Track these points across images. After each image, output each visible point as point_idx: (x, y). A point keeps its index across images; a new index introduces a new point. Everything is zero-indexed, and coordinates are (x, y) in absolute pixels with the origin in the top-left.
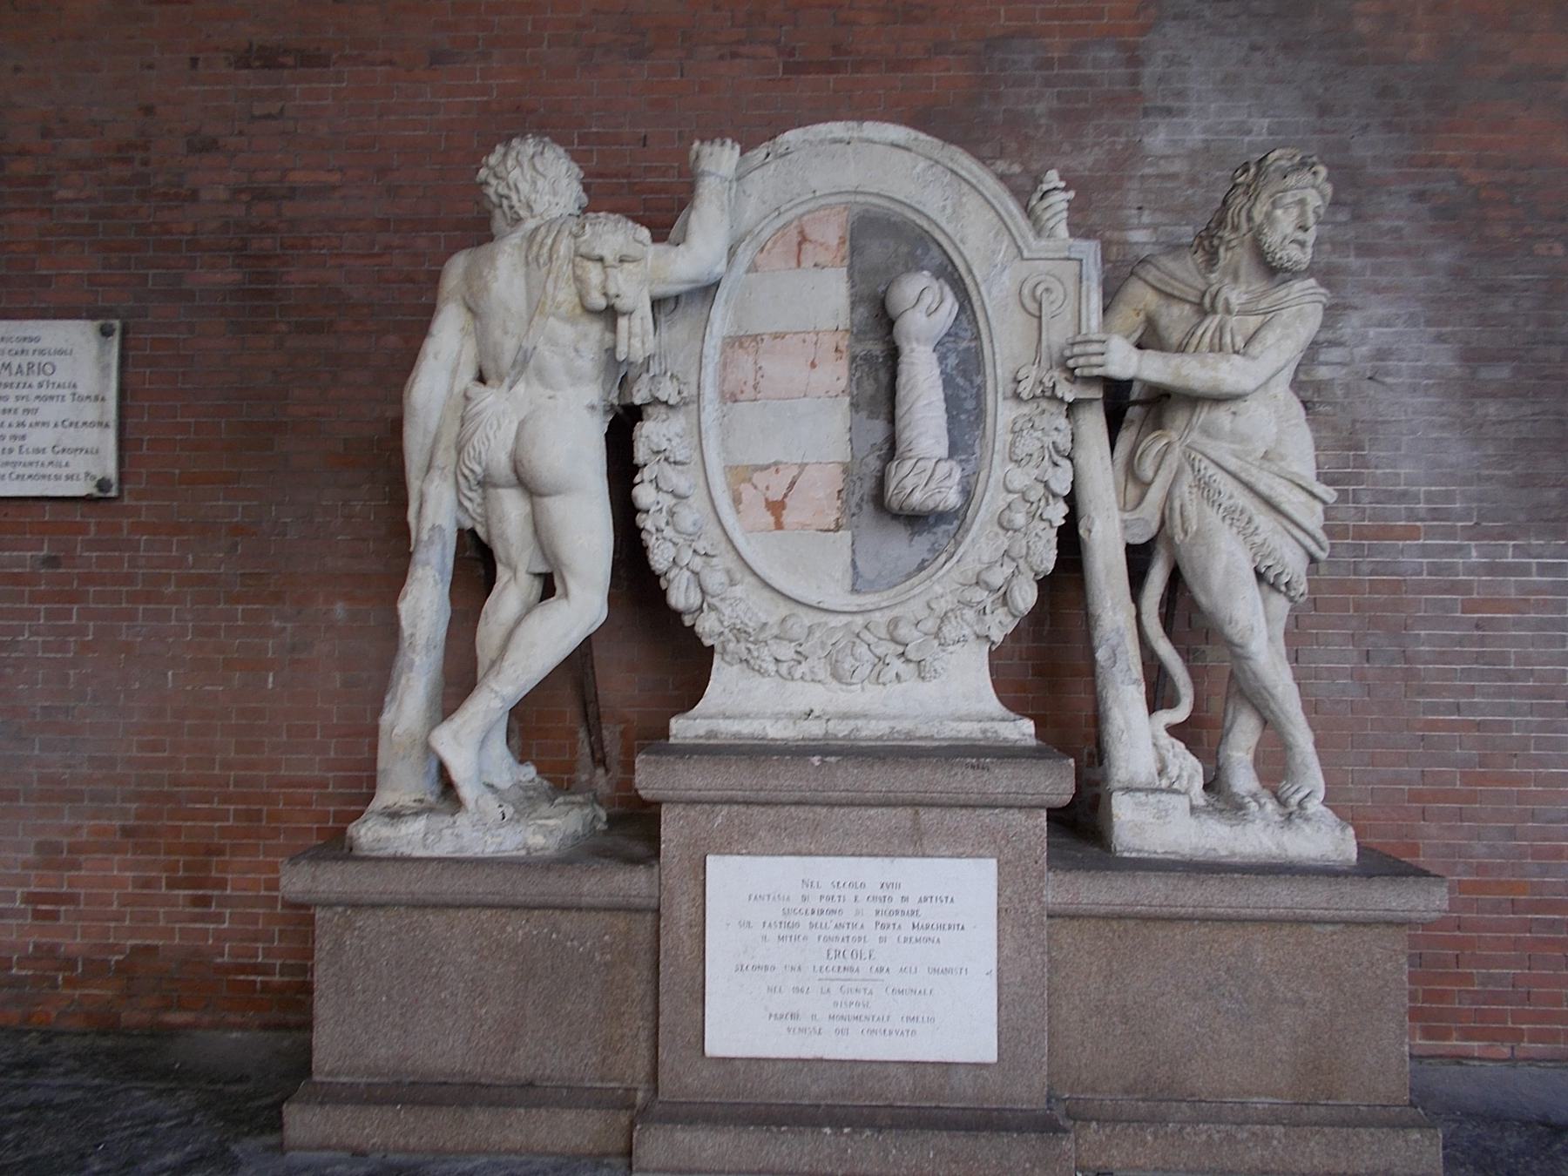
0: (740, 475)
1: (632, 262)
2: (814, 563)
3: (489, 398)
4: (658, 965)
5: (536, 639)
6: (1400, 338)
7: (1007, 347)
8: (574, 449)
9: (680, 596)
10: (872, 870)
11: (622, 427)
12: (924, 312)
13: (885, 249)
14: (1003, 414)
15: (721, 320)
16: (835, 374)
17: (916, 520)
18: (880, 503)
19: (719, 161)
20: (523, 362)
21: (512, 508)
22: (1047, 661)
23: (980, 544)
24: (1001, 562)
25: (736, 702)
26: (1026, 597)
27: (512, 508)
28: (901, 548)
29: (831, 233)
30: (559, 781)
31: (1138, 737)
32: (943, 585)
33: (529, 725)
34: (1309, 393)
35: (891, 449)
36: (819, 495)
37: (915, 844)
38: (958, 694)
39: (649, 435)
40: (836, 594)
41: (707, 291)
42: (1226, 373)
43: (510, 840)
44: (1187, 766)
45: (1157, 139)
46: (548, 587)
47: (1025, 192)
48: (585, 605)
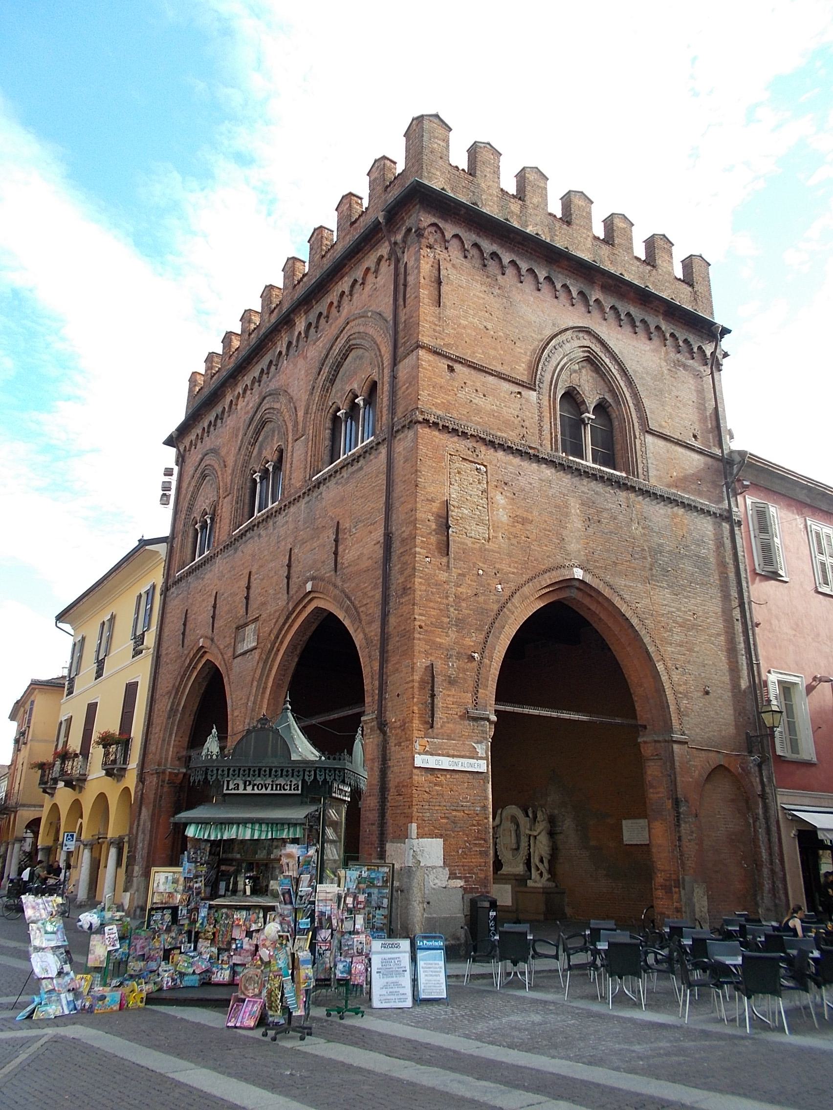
44: (538, 877)
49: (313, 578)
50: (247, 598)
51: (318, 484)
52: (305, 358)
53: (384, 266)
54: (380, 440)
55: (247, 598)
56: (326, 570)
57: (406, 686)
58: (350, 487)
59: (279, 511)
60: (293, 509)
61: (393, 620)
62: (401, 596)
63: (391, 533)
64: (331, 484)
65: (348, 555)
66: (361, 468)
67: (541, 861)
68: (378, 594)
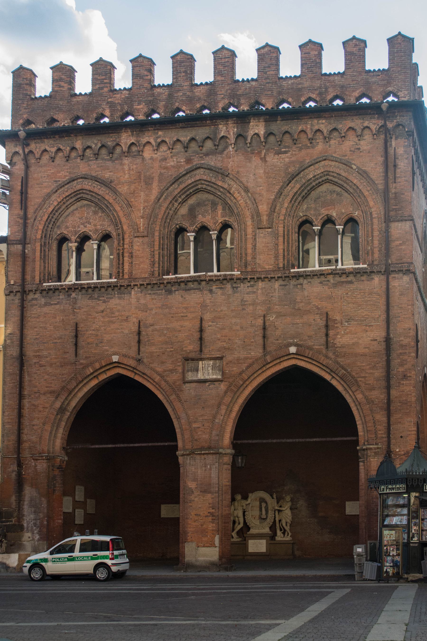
0: (252, 516)
1: (244, 503)
2: (257, 522)
3: (235, 511)
4: (246, 546)
5: (238, 527)
6: (302, 504)
7: (270, 507)
8: (241, 514)
9: (248, 524)
10: (258, 541)
11: (244, 512)
12: (264, 505)
13: (262, 500)
14: (270, 511)
15: (251, 505)
16: (258, 509)
17: (264, 519)
18: (260, 518)
19: (250, 495)
20: (237, 509)
21: (237, 518)
22: (273, 528)
23: (268, 520)
24: (270, 521)
25: (253, 531)
26: (271, 524)
27: (237, 518)
28: (263, 521)
29: (258, 499)
30: (240, 537)
31: (279, 533)
32: (266, 523)
33: (238, 533)
34: (291, 509)
35: (262, 514)
36: (257, 517)
37: (261, 539)
38: (267, 530)
39: (246, 513)
40: (259, 524)
41: (249, 504)
42: (283, 509)
43: (237, 540)
44: (282, 535)
45: (285, 488)
46: (239, 524)
47: (272, 496)
48: (241, 525)
49: (296, 345)
50: (201, 339)
51: (298, 276)
52: (264, 160)
53: (368, 136)
54: (375, 271)
55: (201, 339)
56: (317, 343)
57: (409, 433)
58: (340, 291)
59: (242, 280)
60: (260, 284)
61: (393, 393)
62: (402, 379)
63: (390, 339)
64: (316, 281)
65: (342, 339)
66: (351, 282)
67: (286, 525)
68: (379, 373)
